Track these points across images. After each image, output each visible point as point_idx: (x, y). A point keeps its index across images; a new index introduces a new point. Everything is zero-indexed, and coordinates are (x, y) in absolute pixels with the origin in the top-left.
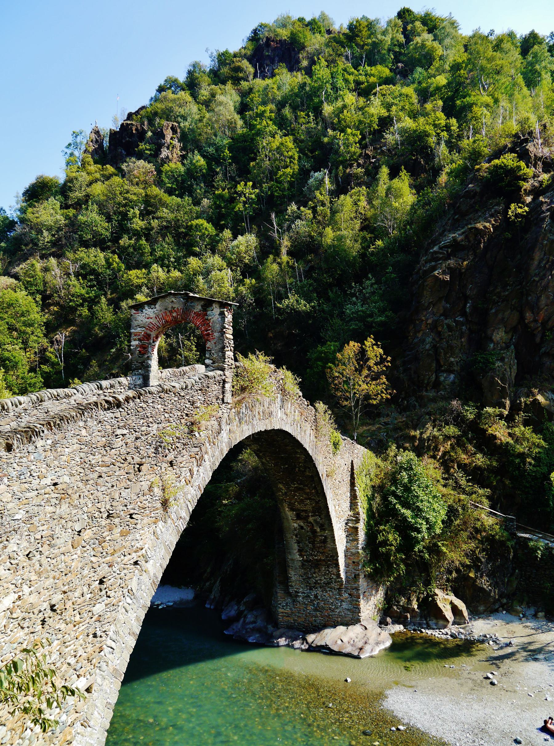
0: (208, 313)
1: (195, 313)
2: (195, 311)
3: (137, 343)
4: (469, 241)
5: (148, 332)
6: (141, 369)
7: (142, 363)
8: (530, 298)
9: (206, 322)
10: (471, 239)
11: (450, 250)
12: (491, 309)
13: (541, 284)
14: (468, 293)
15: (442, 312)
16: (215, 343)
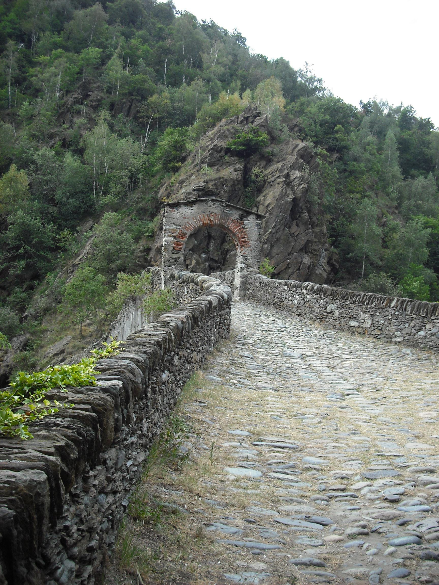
0: (245, 222)
1: (233, 221)
2: (233, 218)
3: (172, 239)
4: (217, 189)
5: (184, 231)
6: (174, 265)
7: (176, 260)
8: (266, 246)
9: (243, 230)
10: (219, 187)
11: (200, 193)
12: (232, 251)
13: (276, 235)
14: (213, 234)
15: (191, 247)
16: (251, 250)
